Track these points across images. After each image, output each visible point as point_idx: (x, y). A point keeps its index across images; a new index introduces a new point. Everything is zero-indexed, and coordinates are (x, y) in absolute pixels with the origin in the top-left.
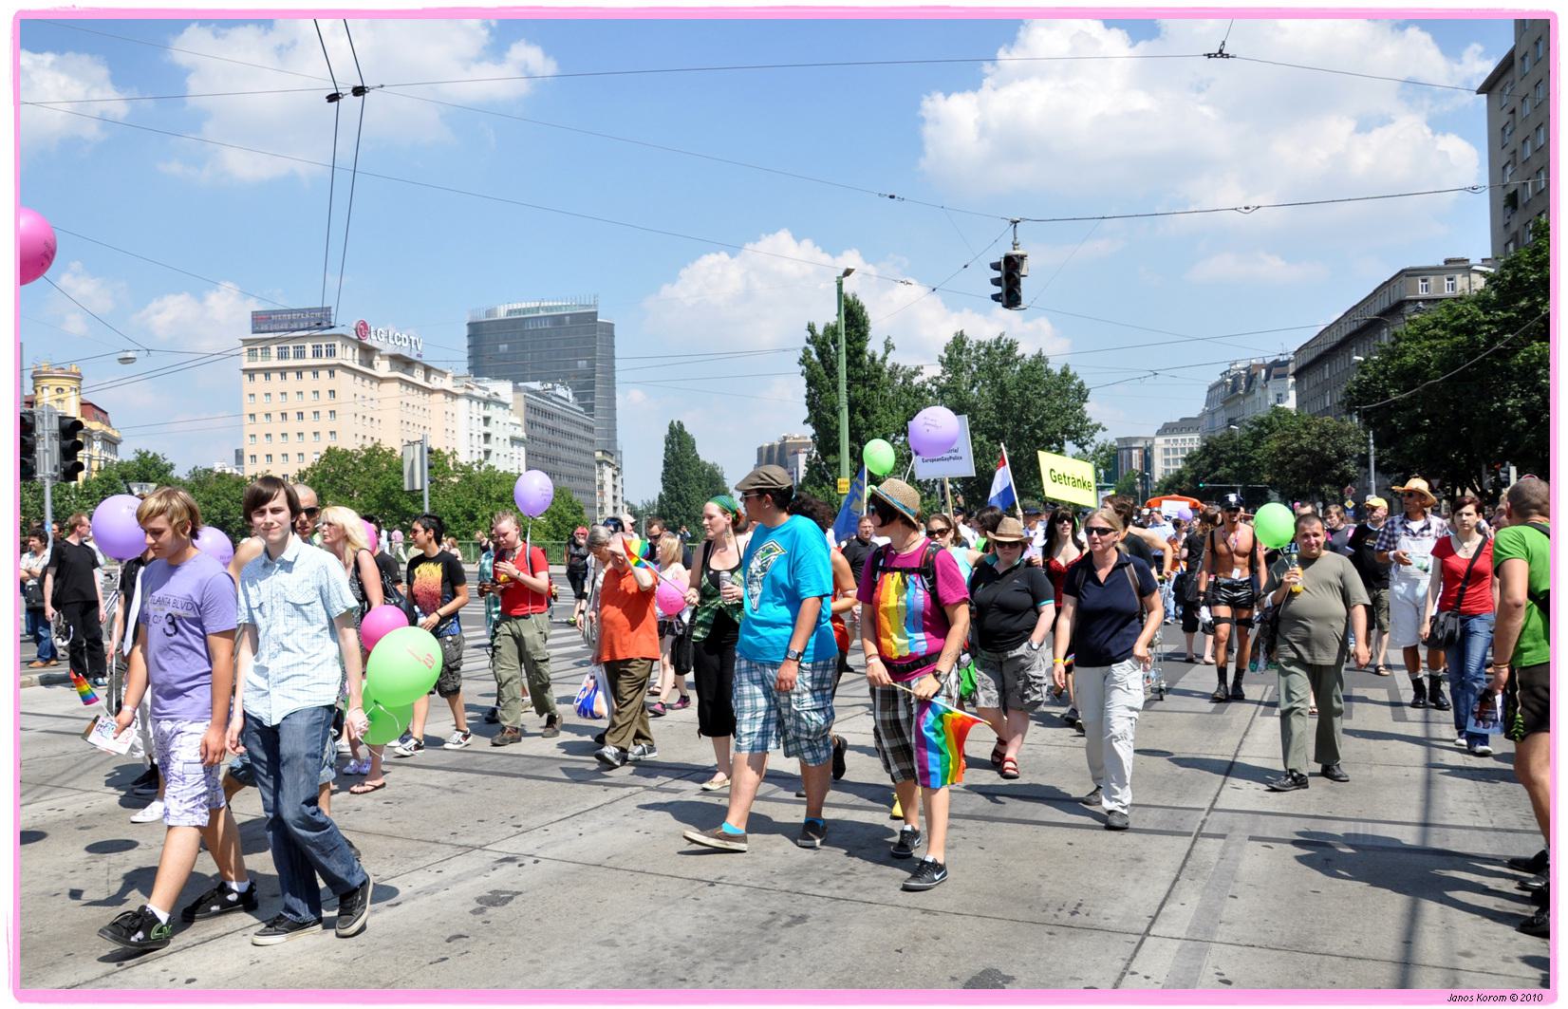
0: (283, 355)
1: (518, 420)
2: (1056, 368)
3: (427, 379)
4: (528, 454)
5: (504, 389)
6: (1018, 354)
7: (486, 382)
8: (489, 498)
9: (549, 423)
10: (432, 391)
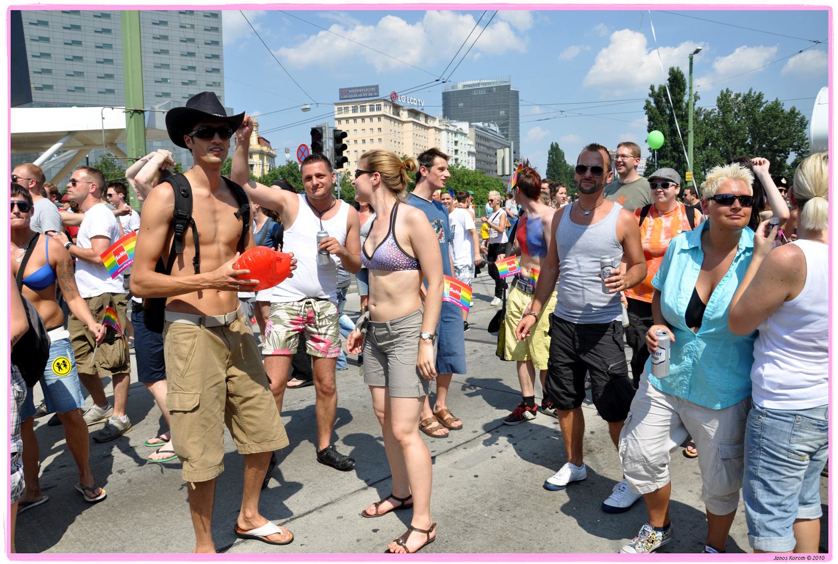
0: (355, 110)
1: (472, 143)
2: (787, 109)
3: (426, 122)
4: (477, 160)
5: (464, 126)
6: (763, 101)
7: (455, 123)
8: (463, 183)
9: (487, 144)
10: (428, 128)
